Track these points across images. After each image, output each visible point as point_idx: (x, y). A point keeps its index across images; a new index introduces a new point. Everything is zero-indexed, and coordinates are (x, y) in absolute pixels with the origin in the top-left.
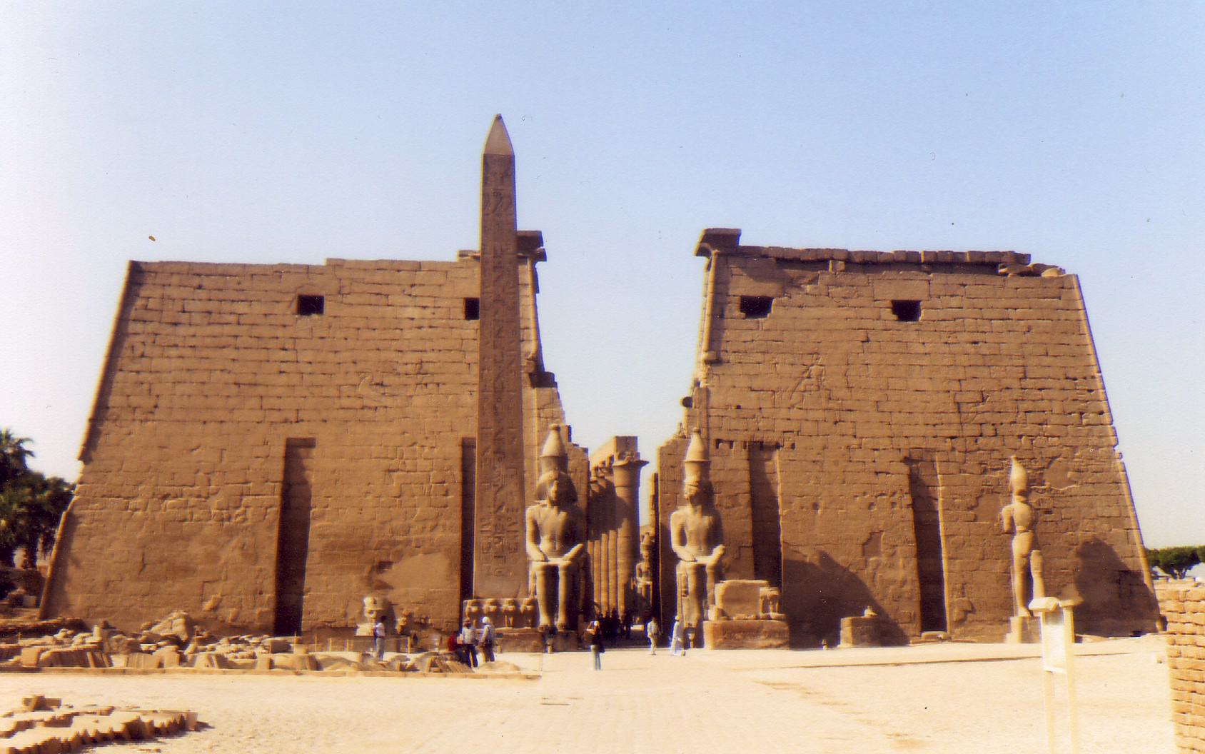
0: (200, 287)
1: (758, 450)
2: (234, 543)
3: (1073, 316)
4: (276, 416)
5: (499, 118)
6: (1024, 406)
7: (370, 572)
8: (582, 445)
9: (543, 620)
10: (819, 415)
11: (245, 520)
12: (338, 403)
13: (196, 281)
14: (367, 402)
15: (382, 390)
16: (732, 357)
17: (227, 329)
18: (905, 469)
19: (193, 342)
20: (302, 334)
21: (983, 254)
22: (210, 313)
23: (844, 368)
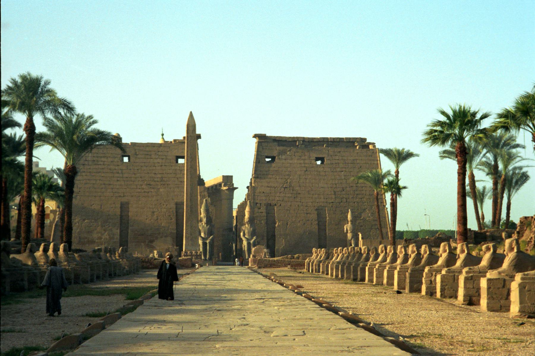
1: (269, 206)
2: (106, 234)
3: (376, 162)
5: (191, 113)
6: (356, 193)
9: (203, 258)
10: (290, 195)
15: (150, 186)
17: (100, 166)
19: (90, 170)
20: (124, 168)
21: (350, 138)
22: (94, 161)
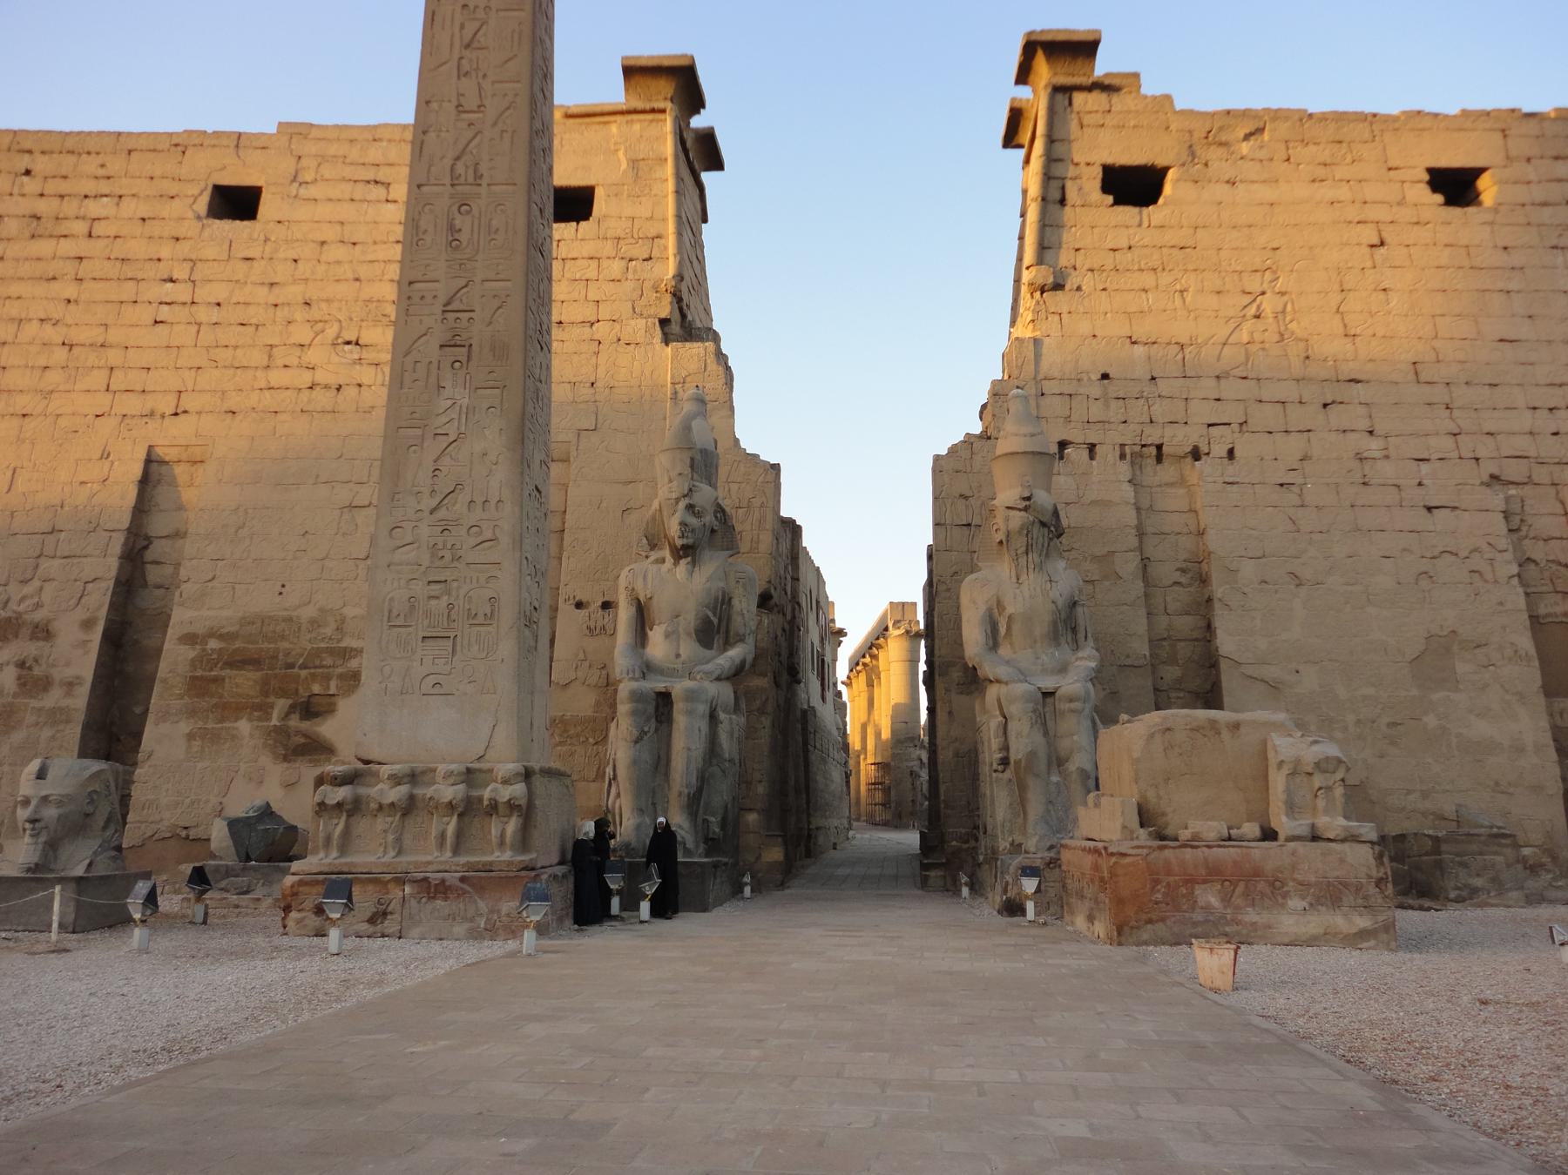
0: (28, 172)
4: (133, 405)
7: (287, 715)
8: (768, 456)
11: (38, 606)
12: (262, 379)
13: (24, 162)
14: (320, 376)
15: (352, 352)
16: (1088, 282)
17: (66, 247)
18: (1496, 499)
20: (210, 252)
23: (1335, 298)
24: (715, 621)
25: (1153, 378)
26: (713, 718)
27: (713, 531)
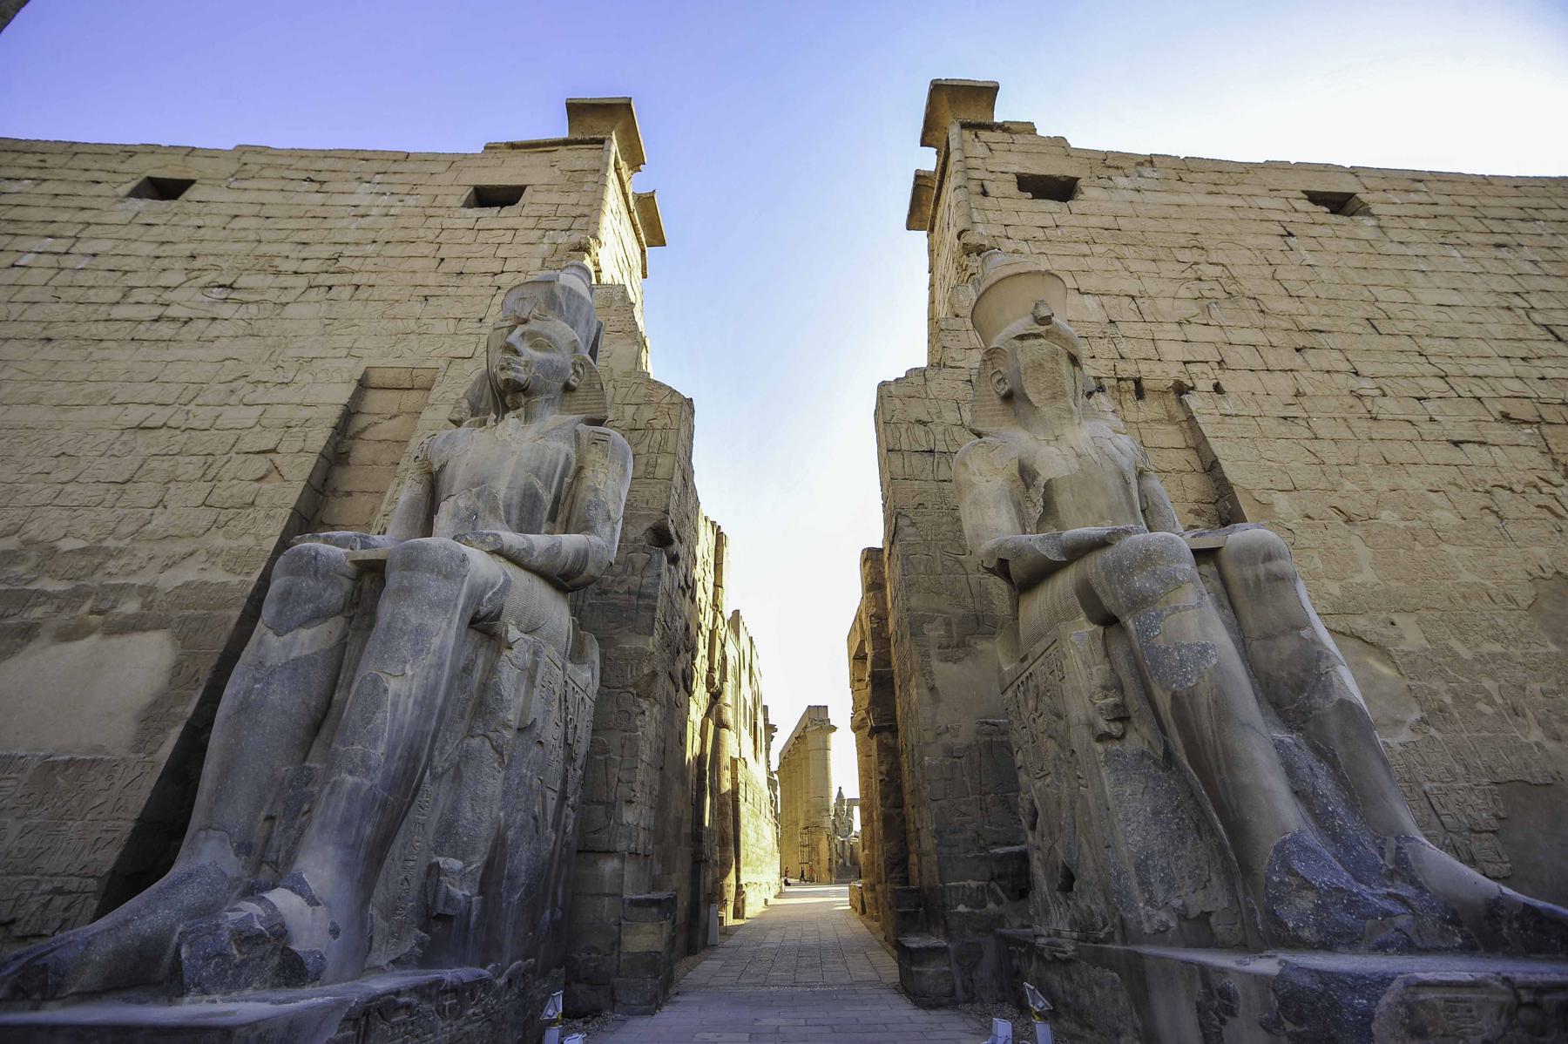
24: (547, 498)
25: (1111, 322)
26: (484, 625)
27: (568, 388)
